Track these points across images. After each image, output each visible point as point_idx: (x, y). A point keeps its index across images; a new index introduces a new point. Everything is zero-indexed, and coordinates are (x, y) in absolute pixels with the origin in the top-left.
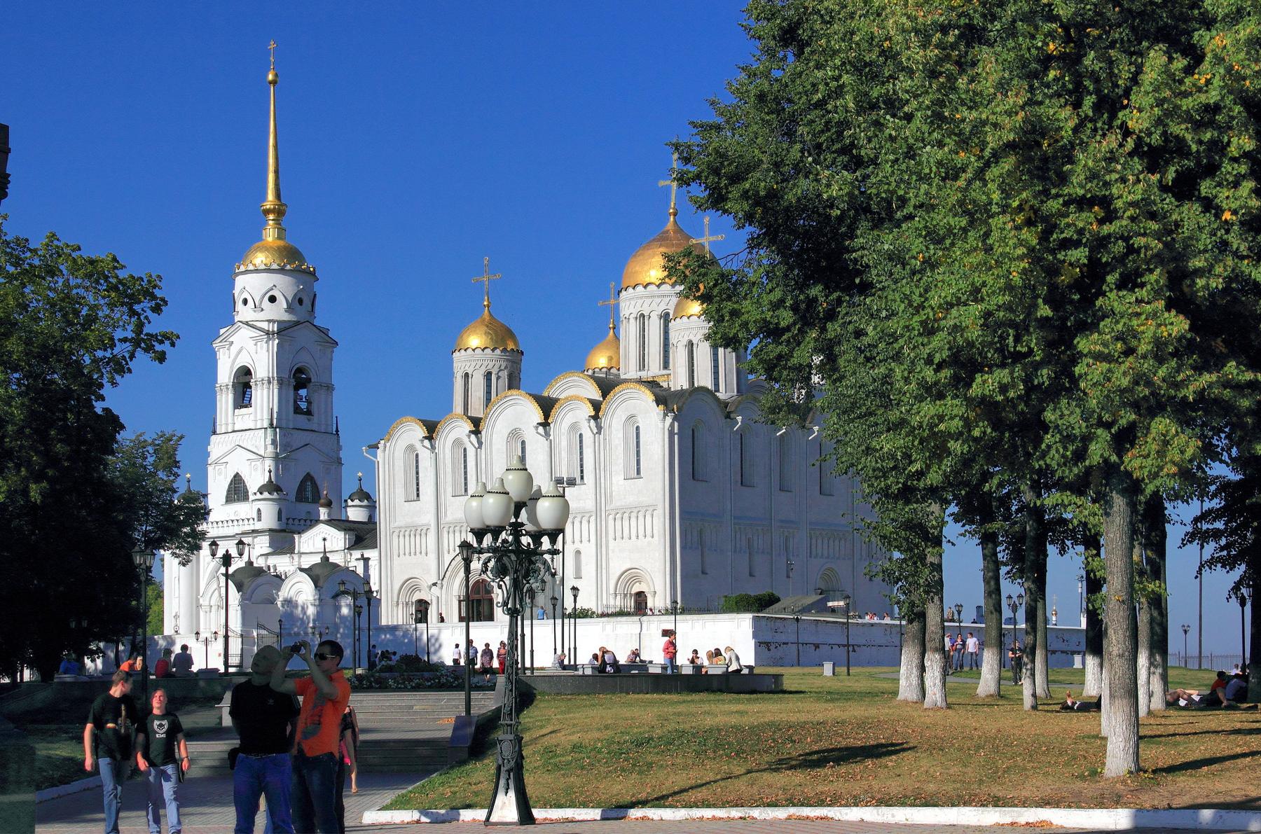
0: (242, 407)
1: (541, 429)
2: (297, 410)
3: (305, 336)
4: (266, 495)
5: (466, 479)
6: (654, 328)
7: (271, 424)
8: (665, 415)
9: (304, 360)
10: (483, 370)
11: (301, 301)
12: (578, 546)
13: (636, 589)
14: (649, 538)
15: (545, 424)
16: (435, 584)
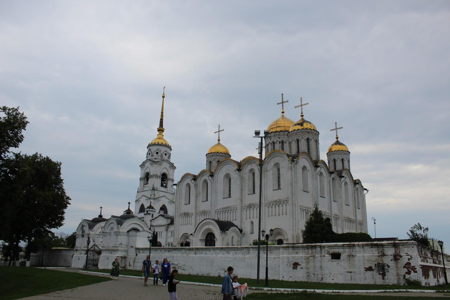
0: (147, 184)
2: (162, 185)
3: (165, 165)
4: (148, 209)
5: (207, 194)
7: (153, 189)
9: (165, 171)
10: (216, 160)
11: (166, 154)
12: (252, 219)
13: (279, 237)
14: (284, 215)
15: (239, 170)
16: (191, 234)
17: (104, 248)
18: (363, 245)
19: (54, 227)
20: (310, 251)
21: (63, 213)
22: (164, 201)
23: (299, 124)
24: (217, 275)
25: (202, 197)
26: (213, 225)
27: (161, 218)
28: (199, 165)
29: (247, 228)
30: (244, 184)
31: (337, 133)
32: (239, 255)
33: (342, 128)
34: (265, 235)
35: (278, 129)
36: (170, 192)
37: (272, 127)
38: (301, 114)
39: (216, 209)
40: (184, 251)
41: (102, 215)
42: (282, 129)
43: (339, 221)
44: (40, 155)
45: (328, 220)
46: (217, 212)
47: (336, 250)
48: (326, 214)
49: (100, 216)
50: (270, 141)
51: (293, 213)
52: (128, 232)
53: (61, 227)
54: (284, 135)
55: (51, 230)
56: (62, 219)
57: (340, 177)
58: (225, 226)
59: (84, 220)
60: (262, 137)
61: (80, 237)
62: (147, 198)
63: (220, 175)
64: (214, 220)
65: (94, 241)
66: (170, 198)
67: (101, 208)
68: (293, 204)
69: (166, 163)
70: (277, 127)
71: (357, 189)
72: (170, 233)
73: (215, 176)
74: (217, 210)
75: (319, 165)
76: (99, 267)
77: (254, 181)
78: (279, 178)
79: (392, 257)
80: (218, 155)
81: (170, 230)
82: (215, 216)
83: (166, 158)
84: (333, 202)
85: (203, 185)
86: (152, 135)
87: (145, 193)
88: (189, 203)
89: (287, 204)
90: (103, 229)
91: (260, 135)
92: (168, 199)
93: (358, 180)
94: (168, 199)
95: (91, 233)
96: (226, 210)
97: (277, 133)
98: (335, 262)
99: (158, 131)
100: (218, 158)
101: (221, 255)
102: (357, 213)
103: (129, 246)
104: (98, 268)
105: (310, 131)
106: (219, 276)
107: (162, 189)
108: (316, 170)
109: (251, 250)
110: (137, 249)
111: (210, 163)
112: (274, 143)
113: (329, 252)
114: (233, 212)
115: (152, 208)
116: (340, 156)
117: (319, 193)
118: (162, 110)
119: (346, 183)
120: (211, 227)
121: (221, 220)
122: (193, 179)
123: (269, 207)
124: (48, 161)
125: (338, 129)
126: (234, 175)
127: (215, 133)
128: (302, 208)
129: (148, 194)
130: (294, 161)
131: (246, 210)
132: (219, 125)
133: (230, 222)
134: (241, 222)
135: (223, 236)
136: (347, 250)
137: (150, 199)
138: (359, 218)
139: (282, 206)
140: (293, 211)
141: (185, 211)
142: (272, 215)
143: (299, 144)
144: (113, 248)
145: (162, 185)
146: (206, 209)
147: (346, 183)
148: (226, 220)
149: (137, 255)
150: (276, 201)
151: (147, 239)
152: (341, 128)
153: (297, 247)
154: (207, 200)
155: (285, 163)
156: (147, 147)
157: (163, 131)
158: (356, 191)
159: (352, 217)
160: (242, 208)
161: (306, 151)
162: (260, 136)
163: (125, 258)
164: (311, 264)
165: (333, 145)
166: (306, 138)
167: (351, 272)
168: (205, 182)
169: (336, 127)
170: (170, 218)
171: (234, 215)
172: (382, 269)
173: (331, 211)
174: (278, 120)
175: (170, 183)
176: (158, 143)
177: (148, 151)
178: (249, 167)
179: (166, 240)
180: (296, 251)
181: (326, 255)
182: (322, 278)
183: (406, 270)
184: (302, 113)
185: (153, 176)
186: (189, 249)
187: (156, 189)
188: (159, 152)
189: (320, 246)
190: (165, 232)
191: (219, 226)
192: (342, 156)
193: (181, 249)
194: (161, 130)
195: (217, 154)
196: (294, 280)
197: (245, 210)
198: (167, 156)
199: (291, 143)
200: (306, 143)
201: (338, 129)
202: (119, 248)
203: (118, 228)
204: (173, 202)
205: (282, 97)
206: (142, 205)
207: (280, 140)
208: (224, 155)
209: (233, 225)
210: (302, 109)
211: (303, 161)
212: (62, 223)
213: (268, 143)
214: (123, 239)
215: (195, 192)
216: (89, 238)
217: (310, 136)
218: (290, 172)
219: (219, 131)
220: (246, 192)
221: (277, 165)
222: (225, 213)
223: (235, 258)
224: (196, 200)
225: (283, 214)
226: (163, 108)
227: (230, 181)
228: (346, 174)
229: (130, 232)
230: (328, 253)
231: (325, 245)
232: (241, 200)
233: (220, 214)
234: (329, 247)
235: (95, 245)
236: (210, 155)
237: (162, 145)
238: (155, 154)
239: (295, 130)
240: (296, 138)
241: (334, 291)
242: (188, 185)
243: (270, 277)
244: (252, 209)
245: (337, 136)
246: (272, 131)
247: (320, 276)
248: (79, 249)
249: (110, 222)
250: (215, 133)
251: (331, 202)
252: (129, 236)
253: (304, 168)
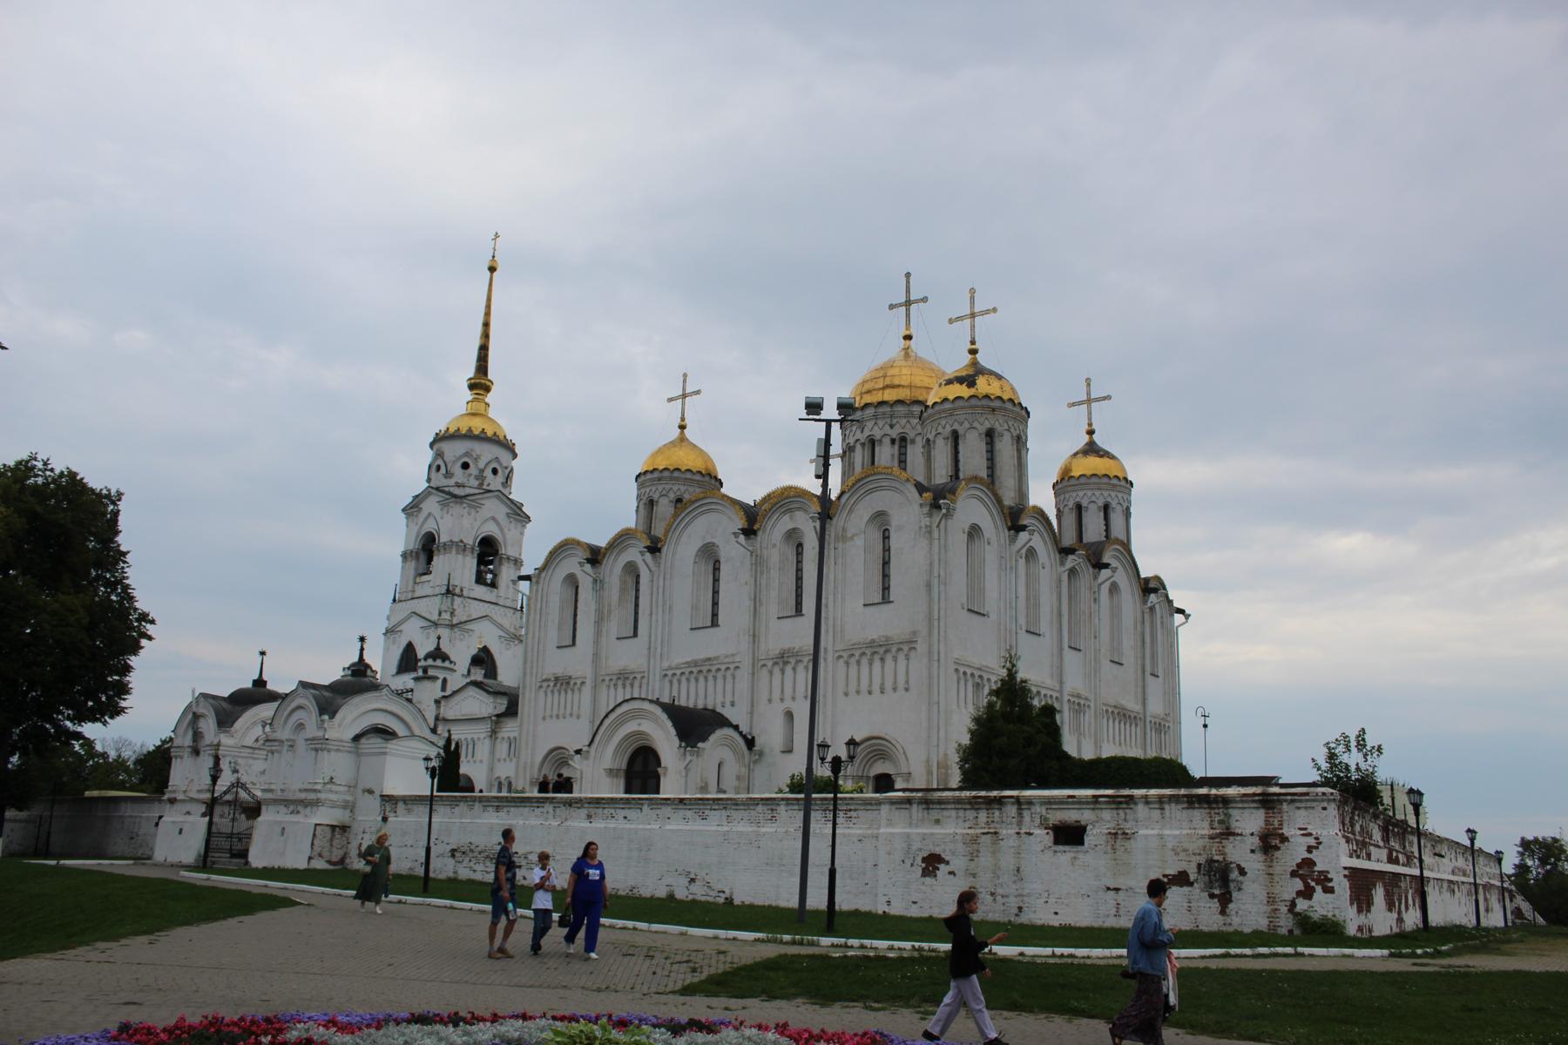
0: (428, 572)
1: (742, 537)
2: (480, 580)
3: (492, 507)
4: (430, 662)
5: (636, 613)
7: (448, 591)
8: (935, 506)
9: (490, 529)
10: (672, 496)
11: (495, 471)
12: (788, 704)
13: (880, 768)
14: (901, 692)
15: (749, 532)
16: (578, 752)
17: (269, 796)
18: (1161, 800)
19: (94, 720)
20: (983, 815)
21: (127, 669)
22: (486, 635)
23: (960, 380)
24: (661, 893)
25: (618, 622)
26: (656, 720)
27: (473, 692)
28: (611, 511)
29: (771, 734)
30: (764, 582)
31: (1090, 413)
32: (741, 825)
33: (1108, 398)
34: (829, 759)
35: (890, 396)
36: (508, 603)
37: (867, 387)
38: (969, 346)
39: (666, 665)
40: (549, 807)
41: (265, 678)
43: (1088, 718)
44: (45, 464)
45: (1049, 711)
46: (668, 676)
47: (1071, 816)
48: (1043, 692)
49: (260, 683)
50: (859, 435)
51: (930, 687)
52: (357, 738)
53: (119, 719)
54: (910, 415)
55: (79, 729)
56: (123, 690)
57: (1094, 566)
58: (694, 726)
59: (205, 696)
60: (829, 422)
61: (186, 753)
62: (426, 624)
63: (684, 549)
64: (657, 702)
65: (235, 771)
66: (506, 622)
67: (263, 653)
68: (930, 653)
69: (496, 502)
70: (884, 388)
71: (1152, 609)
72: (505, 745)
73: (664, 550)
74: (670, 668)
75: (1025, 521)
76: (251, 859)
77: (799, 570)
78: (886, 563)
79: (1255, 841)
80: (677, 479)
81: (506, 735)
82: (661, 689)
83: (495, 483)
84: (1069, 655)
85: (623, 582)
86: (452, 404)
87: (422, 607)
88: (574, 644)
89: (912, 654)
90: (268, 728)
91: (824, 415)
92: (500, 626)
93: (1157, 578)
94: (500, 626)
95: (225, 740)
96: (701, 669)
97: (887, 409)
98: (1066, 854)
99: (472, 387)
100: (678, 488)
101: (679, 825)
102: (1149, 690)
103: (361, 786)
104: (247, 863)
105: (997, 404)
106: (671, 897)
107: (481, 591)
108: (1013, 540)
109: (782, 808)
110: (387, 799)
111: (648, 505)
112: (872, 443)
113: (1046, 819)
114: (725, 678)
115: (445, 657)
116: (1097, 493)
117: (1022, 621)
118: (488, 314)
119: (1114, 589)
120: (646, 726)
121: (683, 703)
122: (589, 561)
123: (847, 663)
124: (72, 486)
125: (1097, 400)
126: (733, 551)
127: (670, 400)
128: (962, 669)
129: (430, 608)
130: (939, 507)
131: (771, 673)
132: (685, 375)
133: (714, 711)
134: (752, 713)
135: (689, 758)
136: (1107, 815)
137: (436, 625)
138: (1155, 707)
139: (895, 659)
140: (930, 677)
141: (559, 671)
142: (858, 692)
143: (961, 448)
144: (303, 796)
145: (480, 580)
146: (632, 666)
147: (1114, 589)
148: (700, 706)
149: (385, 819)
150: (873, 641)
151: (422, 764)
152: (1104, 398)
153: (940, 802)
154: (635, 635)
155: (907, 511)
156: (432, 445)
157: (488, 389)
158: (1147, 616)
159: (1133, 705)
160: (756, 665)
161: (984, 474)
162: (822, 416)
163: (344, 828)
164: (985, 860)
165: (1075, 454)
166: (983, 429)
167: (1117, 890)
168: (632, 570)
169: (1089, 393)
170: (504, 694)
171: (729, 687)
172: (1220, 879)
173: (1061, 683)
174: (890, 365)
175: (506, 573)
176: (470, 430)
177: (435, 459)
178: (785, 523)
179: (492, 769)
180: (935, 814)
181: (1037, 832)
182: (1020, 909)
183: (1298, 884)
184: (973, 342)
185: (447, 547)
186: (569, 803)
187: (457, 591)
188: (471, 462)
189: (1018, 801)
190: (487, 741)
191: (675, 725)
192: (1106, 493)
193: (540, 802)
194: (480, 384)
195: (676, 474)
196: (926, 915)
197: (765, 672)
198: (500, 478)
199: (931, 444)
200: (983, 446)
201: (1097, 400)
202: (322, 796)
203: (321, 726)
204: (517, 638)
205: (908, 282)
206: (410, 648)
207: (894, 433)
208: (698, 477)
209: (723, 722)
210: (973, 327)
211: (971, 509)
212: (123, 704)
213: (851, 441)
214: (337, 765)
215: (593, 607)
216: (217, 759)
217: (998, 423)
218: (924, 542)
219: (684, 396)
220: (772, 609)
221: (880, 518)
222: (697, 680)
223: (726, 833)
224: (598, 634)
225: (895, 689)
226: (488, 307)
227: (716, 569)
228: (1116, 557)
229: (363, 740)
230: (1044, 824)
231: (1035, 797)
233: (679, 682)
234: (1049, 802)
235: (238, 784)
236: (649, 476)
237: (482, 438)
238: (457, 470)
239: (946, 400)
240: (949, 429)
241: (1058, 951)
242: (572, 581)
243: (844, 903)
244: (789, 669)
245: (1090, 425)
246: (868, 399)
247: (1013, 902)
248: (180, 797)
249: (293, 705)
250: (670, 400)
251: (1061, 649)
252: (358, 755)
253: (974, 532)
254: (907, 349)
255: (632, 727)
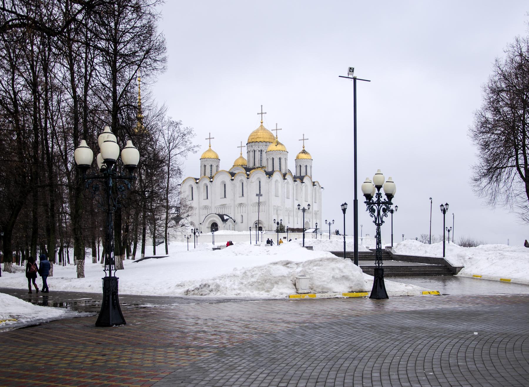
6: (258, 154)
12: (242, 214)
26: (217, 218)
29: (238, 220)
35: (258, 140)
42: (262, 140)
78: (260, 187)
96: (223, 206)
120: (215, 219)
147: (306, 186)
207: (260, 149)
211: (277, 176)
232: (234, 201)
246: (253, 140)
254: (262, 126)
255: (212, 219)
